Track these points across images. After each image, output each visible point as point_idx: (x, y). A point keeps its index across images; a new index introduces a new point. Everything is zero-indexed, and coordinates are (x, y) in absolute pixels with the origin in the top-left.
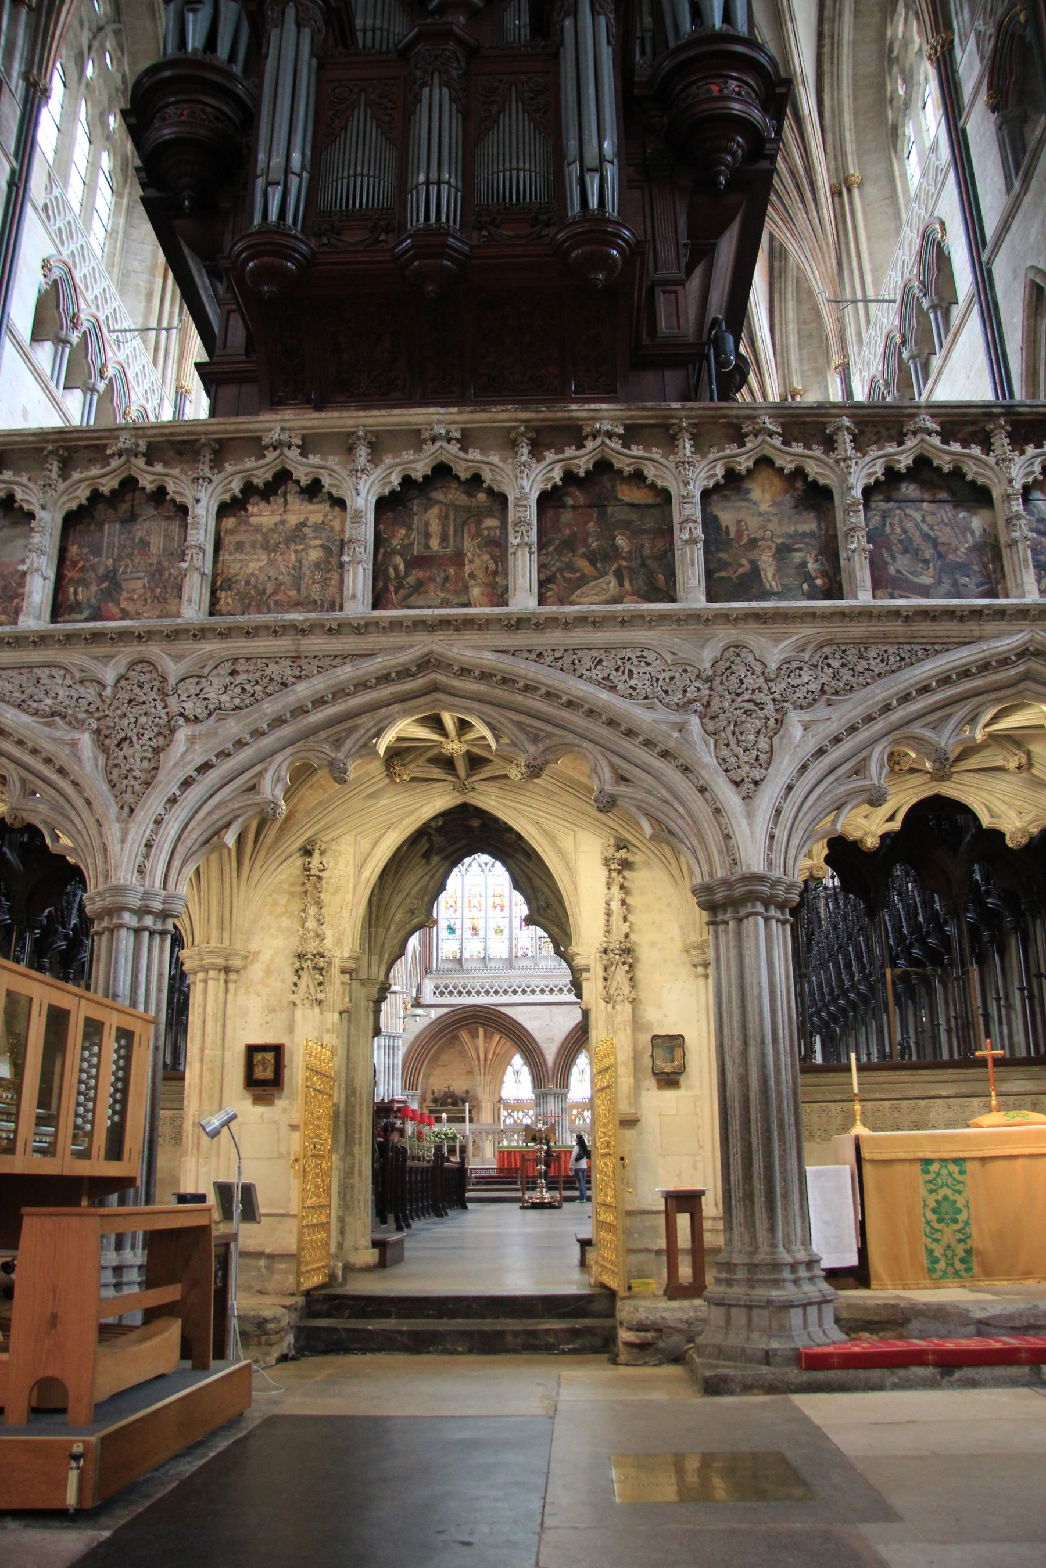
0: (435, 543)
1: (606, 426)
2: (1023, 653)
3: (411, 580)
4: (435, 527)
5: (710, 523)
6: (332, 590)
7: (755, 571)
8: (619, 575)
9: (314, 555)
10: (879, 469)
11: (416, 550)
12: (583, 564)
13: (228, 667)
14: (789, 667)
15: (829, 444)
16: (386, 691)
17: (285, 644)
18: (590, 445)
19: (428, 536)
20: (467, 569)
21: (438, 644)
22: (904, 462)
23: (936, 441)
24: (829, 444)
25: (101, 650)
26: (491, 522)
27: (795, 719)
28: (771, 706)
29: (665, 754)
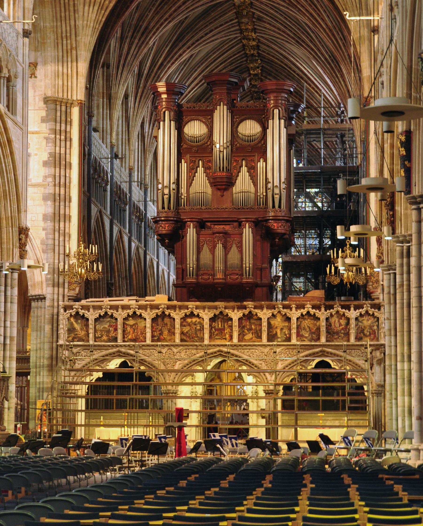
0: (220, 326)
1: (250, 306)
3: (216, 333)
4: (220, 323)
5: (269, 324)
6: (202, 335)
7: (276, 333)
8: (252, 333)
9: (198, 328)
10: (299, 315)
12: (246, 331)
16: (212, 355)
18: (248, 309)
19: (218, 325)
24: (291, 309)
26: (230, 322)
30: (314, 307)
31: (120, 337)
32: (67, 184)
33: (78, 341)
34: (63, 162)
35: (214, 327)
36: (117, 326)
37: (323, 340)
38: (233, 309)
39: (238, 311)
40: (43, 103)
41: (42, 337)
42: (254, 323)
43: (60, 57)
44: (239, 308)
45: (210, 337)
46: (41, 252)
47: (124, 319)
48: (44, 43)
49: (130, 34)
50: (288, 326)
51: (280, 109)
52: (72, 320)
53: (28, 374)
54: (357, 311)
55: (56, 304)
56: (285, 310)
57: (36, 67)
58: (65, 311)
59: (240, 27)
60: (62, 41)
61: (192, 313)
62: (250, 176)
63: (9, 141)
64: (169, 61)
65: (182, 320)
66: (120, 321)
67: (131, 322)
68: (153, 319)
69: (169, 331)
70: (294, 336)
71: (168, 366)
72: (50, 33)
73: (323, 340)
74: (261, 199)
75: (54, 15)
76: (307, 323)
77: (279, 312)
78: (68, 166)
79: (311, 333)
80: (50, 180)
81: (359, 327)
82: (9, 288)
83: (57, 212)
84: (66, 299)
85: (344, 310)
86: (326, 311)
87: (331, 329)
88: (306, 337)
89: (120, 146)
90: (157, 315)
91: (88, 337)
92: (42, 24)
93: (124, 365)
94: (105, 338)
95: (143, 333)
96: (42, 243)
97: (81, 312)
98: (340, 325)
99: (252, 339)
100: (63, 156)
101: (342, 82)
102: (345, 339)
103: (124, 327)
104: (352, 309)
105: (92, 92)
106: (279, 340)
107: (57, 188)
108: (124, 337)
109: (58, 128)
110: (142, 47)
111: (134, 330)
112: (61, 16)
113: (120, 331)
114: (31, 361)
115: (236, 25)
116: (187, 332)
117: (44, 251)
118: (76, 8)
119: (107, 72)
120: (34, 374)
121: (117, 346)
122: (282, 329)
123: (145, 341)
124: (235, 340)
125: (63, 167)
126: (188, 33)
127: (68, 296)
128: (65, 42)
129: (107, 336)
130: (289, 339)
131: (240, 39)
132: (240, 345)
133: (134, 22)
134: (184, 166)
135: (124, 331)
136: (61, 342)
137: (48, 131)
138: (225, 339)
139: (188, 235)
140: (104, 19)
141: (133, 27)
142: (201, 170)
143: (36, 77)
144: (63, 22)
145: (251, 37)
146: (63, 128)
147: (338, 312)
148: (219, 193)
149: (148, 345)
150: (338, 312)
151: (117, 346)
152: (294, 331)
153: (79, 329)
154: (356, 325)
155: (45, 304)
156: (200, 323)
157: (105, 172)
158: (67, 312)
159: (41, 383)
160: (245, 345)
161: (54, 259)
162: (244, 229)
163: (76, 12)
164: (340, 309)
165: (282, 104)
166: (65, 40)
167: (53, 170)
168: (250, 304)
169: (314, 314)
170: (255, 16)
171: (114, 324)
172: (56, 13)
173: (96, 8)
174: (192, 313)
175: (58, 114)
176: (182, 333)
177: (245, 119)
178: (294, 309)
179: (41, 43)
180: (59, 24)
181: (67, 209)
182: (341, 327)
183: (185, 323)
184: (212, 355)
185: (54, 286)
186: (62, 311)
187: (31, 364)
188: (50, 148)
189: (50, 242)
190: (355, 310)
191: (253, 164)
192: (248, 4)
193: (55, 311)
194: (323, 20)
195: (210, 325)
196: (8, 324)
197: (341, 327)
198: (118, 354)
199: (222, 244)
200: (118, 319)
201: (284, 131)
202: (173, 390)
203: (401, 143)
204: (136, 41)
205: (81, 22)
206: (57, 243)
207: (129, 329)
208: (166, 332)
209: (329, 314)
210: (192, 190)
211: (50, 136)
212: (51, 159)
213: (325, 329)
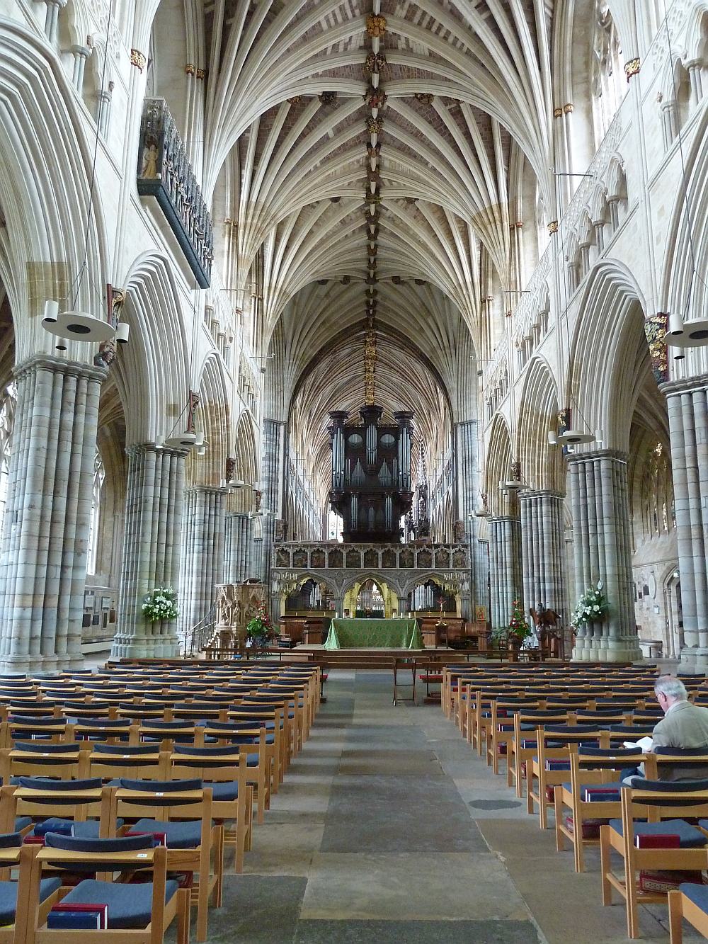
31: (309, 565)
37: (434, 567)
44: (383, 547)
55: (269, 544)
63: (253, 435)
67: (316, 555)
73: (434, 567)
76: (423, 556)
78: (277, 460)
82: (249, 530)
94: (299, 565)
97: (285, 549)
100: (274, 454)
113: (309, 561)
124: (380, 567)
125: (274, 461)
142: (358, 463)
146: (275, 438)
147: (442, 550)
150: (442, 550)
167: (268, 462)
168: (389, 544)
173: (296, 368)
193: (268, 548)
194: (420, 384)
196: (248, 553)
203: (562, 417)
208: (337, 562)
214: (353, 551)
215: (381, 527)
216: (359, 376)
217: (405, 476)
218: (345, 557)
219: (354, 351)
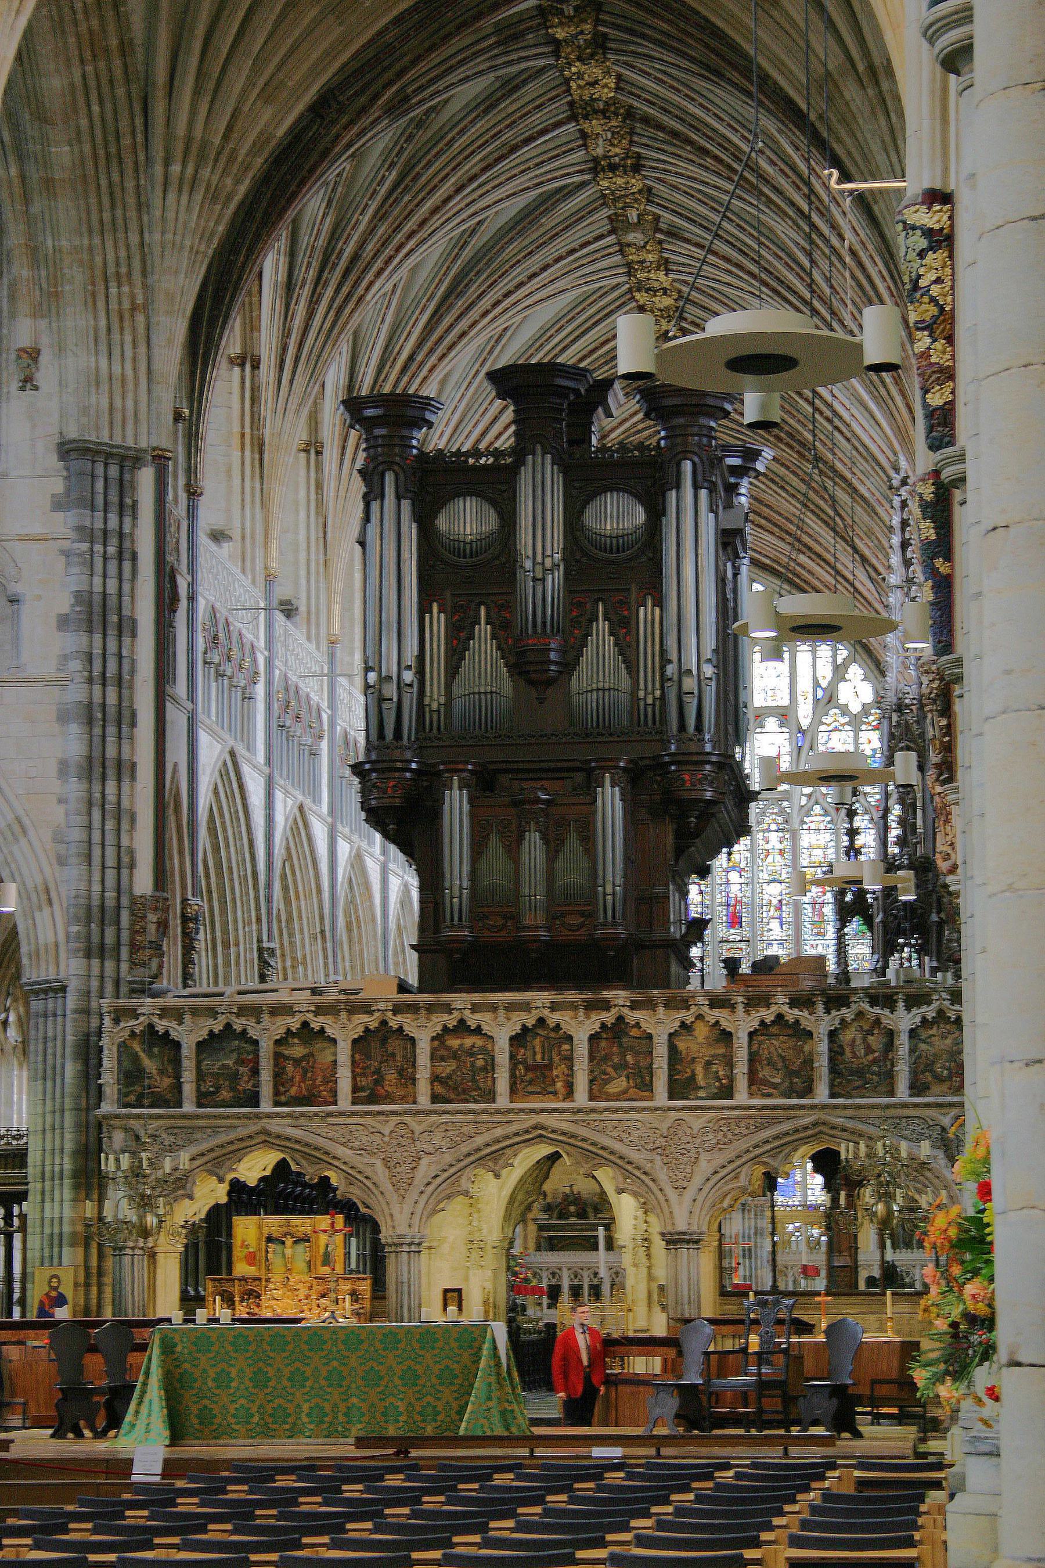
0: (538, 1057)
2: (815, 1124)
3: (527, 1078)
4: (538, 1049)
5: (673, 1050)
6: (490, 1083)
7: (693, 1076)
8: (627, 1077)
9: (480, 1063)
11: (530, 1061)
12: (610, 1070)
13: (443, 1127)
14: (703, 1131)
15: (733, 1007)
16: (518, 1139)
17: (471, 1117)
18: (614, 1010)
19: (535, 1053)
20: (555, 1073)
21: (542, 1118)
22: (769, 1019)
23: (786, 1008)
24: (733, 1007)
25: (381, 1118)
26: (566, 1047)
27: (704, 1157)
28: (693, 1151)
29: (645, 1173)
30: (794, 1003)
31: (266, 1091)
32: (126, 677)
33: (152, 1106)
34: (114, 618)
35: (525, 1060)
36: (257, 1063)
37: (822, 1093)
38: (573, 1007)
39: (588, 1017)
40: (55, 457)
41: (58, 1095)
42: (632, 1048)
43: (103, 332)
44: (591, 1006)
45: (513, 1091)
46: (54, 861)
47: (277, 1042)
48: (57, 295)
49: (312, 273)
50: (723, 1056)
51: (696, 459)
52: (137, 1047)
53: (22, 1197)
54: (915, 1011)
56: (717, 1012)
57: (35, 360)
58: (117, 1021)
59: (623, 256)
60: (107, 288)
61: (462, 1022)
62: (616, 644)
64: (431, 351)
65: (436, 1043)
66: (266, 1048)
67: (297, 1050)
68: (355, 1042)
69: (401, 1072)
70: (741, 1084)
71: (399, 1169)
72: (71, 268)
73: (822, 1093)
74: (650, 709)
75: (84, 216)
76: (775, 1046)
77: (700, 1017)
78: (127, 627)
79: (790, 1074)
80: (76, 665)
81: (920, 1057)
83: (97, 753)
84: (124, 989)
85: (877, 1010)
86: (828, 1012)
87: (843, 1062)
88: (775, 1086)
89: (303, 582)
90: (367, 1030)
91: (180, 1092)
92: (49, 243)
93: (282, 1167)
94: (225, 1094)
95: (331, 1081)
96: (58, 838)
97: (161, 1025)
98: (869, 1050)
99: (625, 1092)
100: (112, 601)
101: (898, 399)
102: (882, 1089)
103: (276, 1065)
104: (901, 1005)
105: (198, 429)
106: (702, 1093)
107: (97, 689)
108: (277, 1093)
109: (99, 524)
110: (348, 311)
111: (306, 1072)
112: (101, 221)
113: (266, 1076)
114: (30, 1160)
115: (612, 250)
116: (449, 1077)
117: (62, 861)
118: (143, 199)
119: (252, 378)
120: (39, 1198)
121: (258, 1117)
122: (709, 1063)
123: (335, 1103)
125: (112, 632)
126: (478, 274)
127: (130, 982)
128: (113, 291)
129: (232, 1089)
130: (727, 1092)
131: (630, 291)
132: (593, 1110)
133: (322, 242)
134: (438, 621)
135: (277, 1076)
136: (107, 1107)
137: (71, 534)
138: (555, 1093)
139: (446, 807)
140: (221, 228)
141: (318, 255)
142: (483, 630)
143: (36, 388)
144: (109, 238)
145: (656, 284)
147: (860, 1014)
148: (533, 693)
149: (342, 1114)
150: (860, 1014)
151: (258, 1117)
152: (741, 1069)
153: (154, 1072)
154: (912, 1051)
155: (64, 1004)
156: (483, 1050)
157: (247, 647)
158: (122, 1025)
159: (56, 1221)
160: (607, 1110)
161: (90, 881)
162: (599, 790)
163: (144, 209)
164: (867, 1007)
165: (699, 445)
166: (113, 284)
167: (84, 638)
168: (619, 996)
169: (797, 1022)
170: (661, 225)
171: (250, 1057)
172: (88, 211)
173: (198, 197)
174: (462, 1022)
175: (100, 486)
176: (435, 1079)
177: (605, 490)
178: (740, 1008)
179: (49, 293)
180: (97, 241)
181: (125, 743)
182: (870, 1057)
183: (443, 1052)
184: (518, 1139)
185: (88, 955)
186: (107, 1021)
187: (30, 1170)
188: (76, 580)
189: (77, 835)
190: (908, 1009)
191: (626, 613)
192: (640, 191)
195: (512, 1057)
197: (870, 1057)
198: (263, 1138)
199: (541, 832)
200: (261, 1044)
201: (708, 523)
202: (413, 1237)
203: (924, 505)
204: (329, 292)
205: (157, 236)
206: (96, 837)
207: (290, 1068)
208: (391, 1077)
209: (837, 1022)
210: (457, 690)
211: (76, 545)
212: (78, 609)
213: (826, 1063)
214: (462, 1027)
215: (574, 920)
216: (565, 193)
217: (690, 684)
218: (423, 1056)
219: (510, 87)
